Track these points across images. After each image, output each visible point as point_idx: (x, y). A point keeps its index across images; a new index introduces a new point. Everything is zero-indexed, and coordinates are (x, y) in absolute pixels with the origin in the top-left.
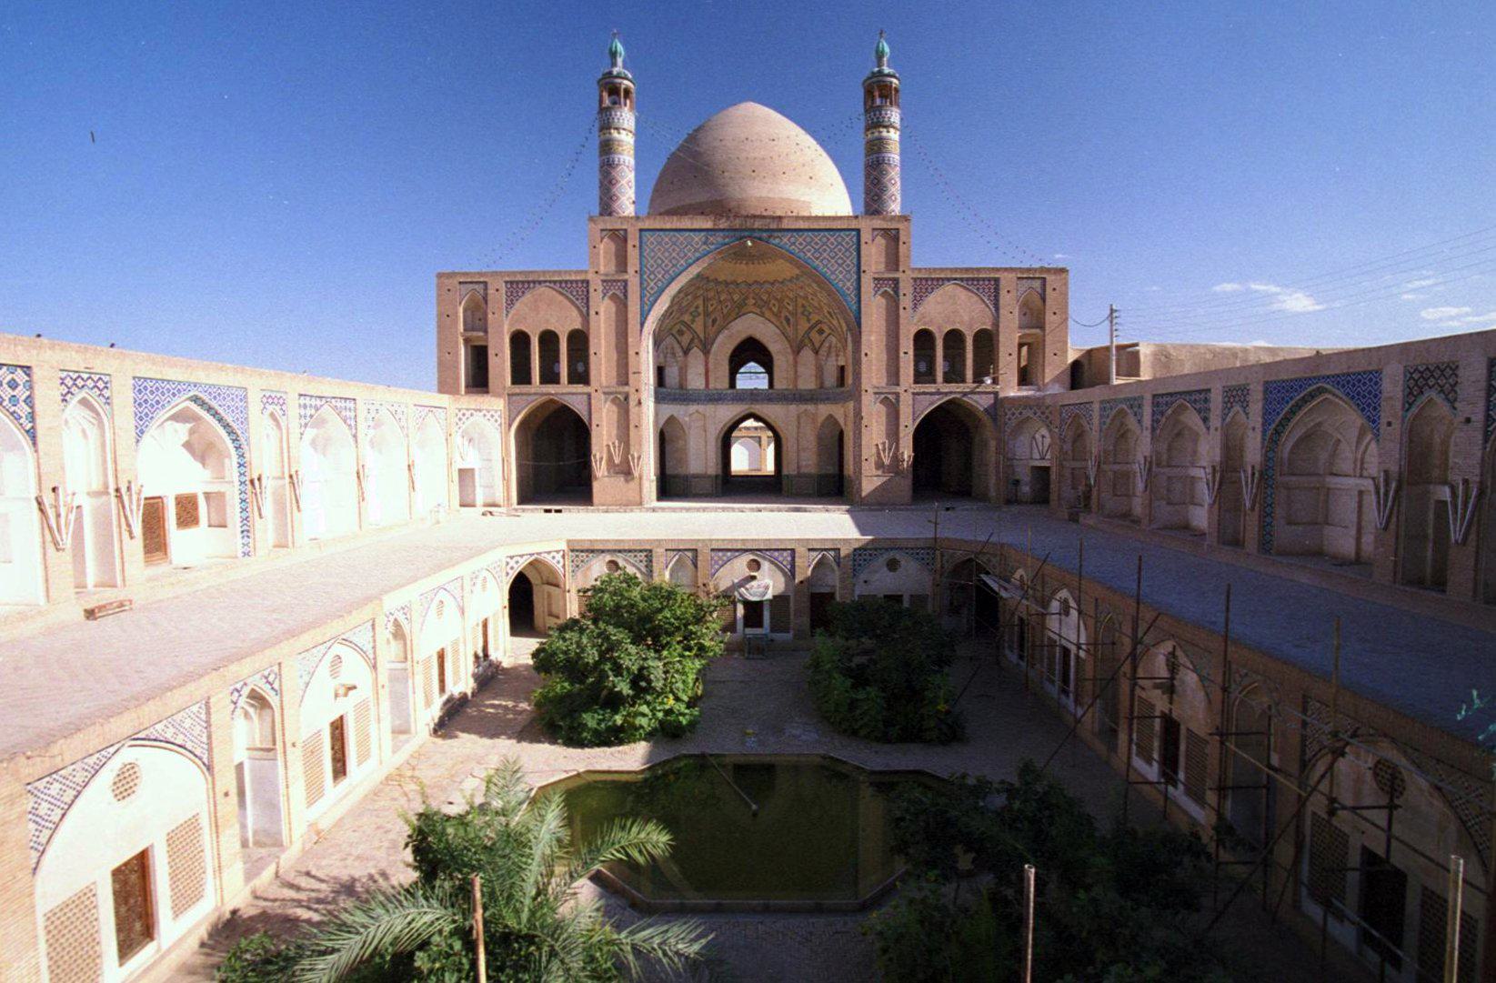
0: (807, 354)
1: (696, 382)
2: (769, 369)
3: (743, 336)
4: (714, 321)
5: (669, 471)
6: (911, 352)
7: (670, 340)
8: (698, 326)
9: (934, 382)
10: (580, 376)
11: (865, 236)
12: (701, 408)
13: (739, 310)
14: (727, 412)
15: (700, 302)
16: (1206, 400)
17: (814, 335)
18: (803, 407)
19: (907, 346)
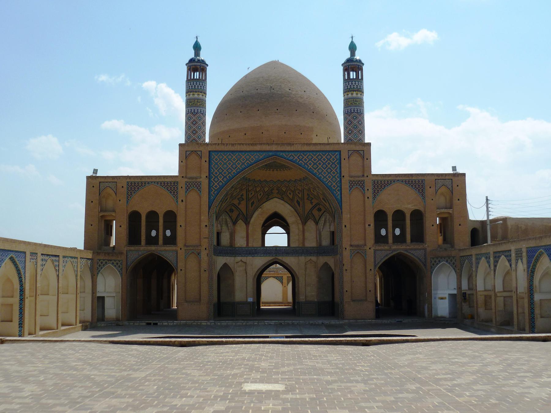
0: (311, 224)
1: (240, 242)
2: (288, 233)
3: (271, 212)
4: (253, 203)
5: (222, 300)
6: (372, 225)
7: (224, 217)
8: (242, 207)
9: (387, 242)
10: (171, 241)
11: (344, 155)
12: (244, 259)
13: (268, 197)
14: (259, 261)
15: (244, 192)
16: (510, 256)
17: (315, 213)
18: (309, 258)
19: (371, 219)
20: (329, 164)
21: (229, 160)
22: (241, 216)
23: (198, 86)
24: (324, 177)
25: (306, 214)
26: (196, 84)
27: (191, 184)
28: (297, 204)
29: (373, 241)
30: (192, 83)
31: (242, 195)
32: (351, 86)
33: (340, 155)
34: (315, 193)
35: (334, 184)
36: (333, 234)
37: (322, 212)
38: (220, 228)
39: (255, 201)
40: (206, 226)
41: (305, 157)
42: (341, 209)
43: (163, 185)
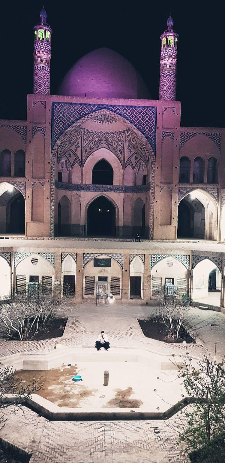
1: (76, 180)
4: (86, 150)
13: (98, 146)
15: (80, 141)
20: (147, 117)
21: (69, 110)
22: (77, 160)
23: (43, 47)
24: (144, 128)
25: (126, 161)
26: (42, 45)
27: (37, 128)
28: (119, 153)
29: (178, 181)
30: (38, 44)
31: (78, 143)
32: (167, 53)
33: (156, 110)
34: (134, 143)
35: (151, 134)
36: (145, 177)
37: (138, 159)
38: (61, 169)
39: (88, 149)
40: (49, 163)
41: (129, 111)
42: (155, 154)
43: (14, 127)
